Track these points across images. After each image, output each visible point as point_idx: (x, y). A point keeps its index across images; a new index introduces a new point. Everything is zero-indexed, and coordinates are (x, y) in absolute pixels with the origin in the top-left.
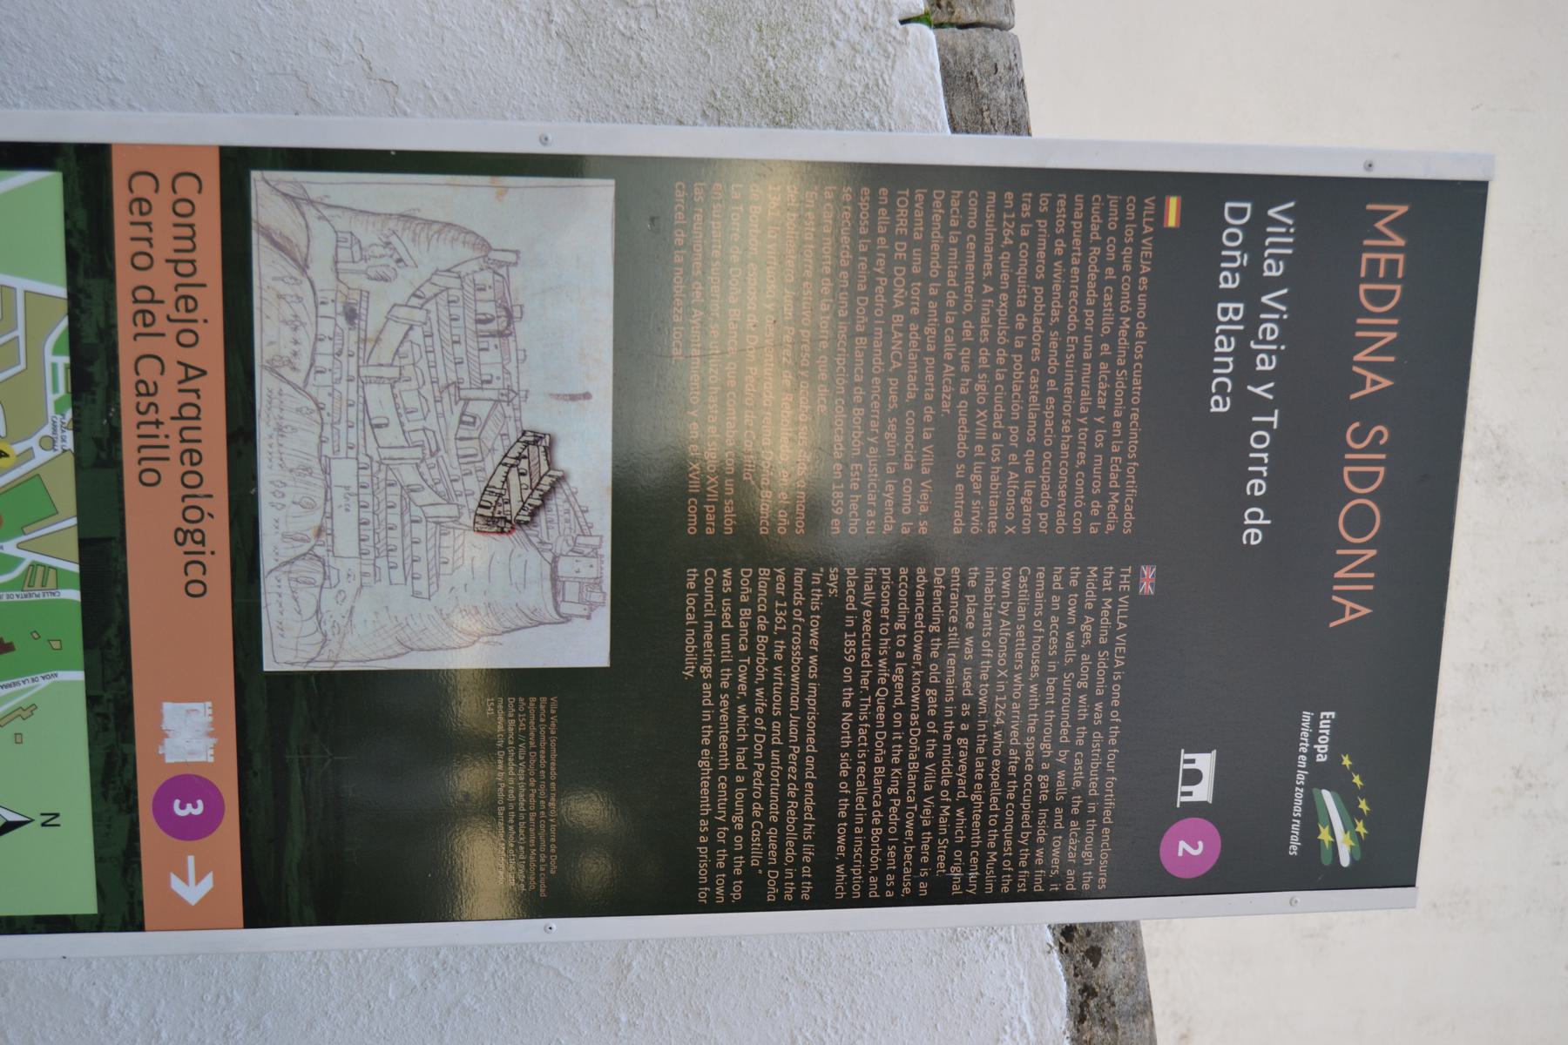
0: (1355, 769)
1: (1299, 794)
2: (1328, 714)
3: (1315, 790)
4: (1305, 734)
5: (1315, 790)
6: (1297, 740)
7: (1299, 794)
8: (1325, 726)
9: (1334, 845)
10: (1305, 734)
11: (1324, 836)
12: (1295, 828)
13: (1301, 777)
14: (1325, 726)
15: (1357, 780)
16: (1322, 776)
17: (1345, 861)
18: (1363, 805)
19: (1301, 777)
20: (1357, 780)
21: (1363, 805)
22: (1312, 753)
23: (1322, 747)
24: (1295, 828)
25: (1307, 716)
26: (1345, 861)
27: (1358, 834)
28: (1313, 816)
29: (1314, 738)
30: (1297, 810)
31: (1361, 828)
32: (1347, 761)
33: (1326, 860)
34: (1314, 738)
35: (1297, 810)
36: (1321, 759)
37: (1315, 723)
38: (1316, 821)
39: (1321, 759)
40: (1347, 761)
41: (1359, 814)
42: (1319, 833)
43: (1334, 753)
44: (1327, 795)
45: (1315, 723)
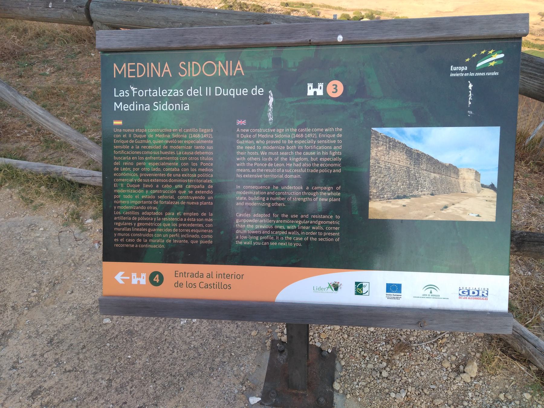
0: (470, 56)
1: (478, 74)
3: (477, 69)
4: (457, 75)
5: (477, 69)
6: (460, 77)
7: (478, 74)
8: (455, 69)
9: (496, 60)
10: (457, 75)
11: (492, 64)
12: (489, 74)
13: (472, 74)
14: (455, 69)
15: (474, 56)
16: (472, 67)
17: (502, 55)
18: (483, 52)
19: (472, 74)
20: (474, 56)
21: (483, 52)
22: (464, 72)
23: (462, 69)
24: (489, 74)
25: (452, 75)
26: (502, 55)
28: (485, 69)
30: (483, 74)
31: (491, 52)
32: (468, 60)
33: (501, 62)
34: (459, 72)
35: (483, 74)
36: (466, 68)
37: (454, 72)
39: (466, 68)
40: (468, 60)
43: (464, 65)
44: (478, 65)
45: (454, 72)
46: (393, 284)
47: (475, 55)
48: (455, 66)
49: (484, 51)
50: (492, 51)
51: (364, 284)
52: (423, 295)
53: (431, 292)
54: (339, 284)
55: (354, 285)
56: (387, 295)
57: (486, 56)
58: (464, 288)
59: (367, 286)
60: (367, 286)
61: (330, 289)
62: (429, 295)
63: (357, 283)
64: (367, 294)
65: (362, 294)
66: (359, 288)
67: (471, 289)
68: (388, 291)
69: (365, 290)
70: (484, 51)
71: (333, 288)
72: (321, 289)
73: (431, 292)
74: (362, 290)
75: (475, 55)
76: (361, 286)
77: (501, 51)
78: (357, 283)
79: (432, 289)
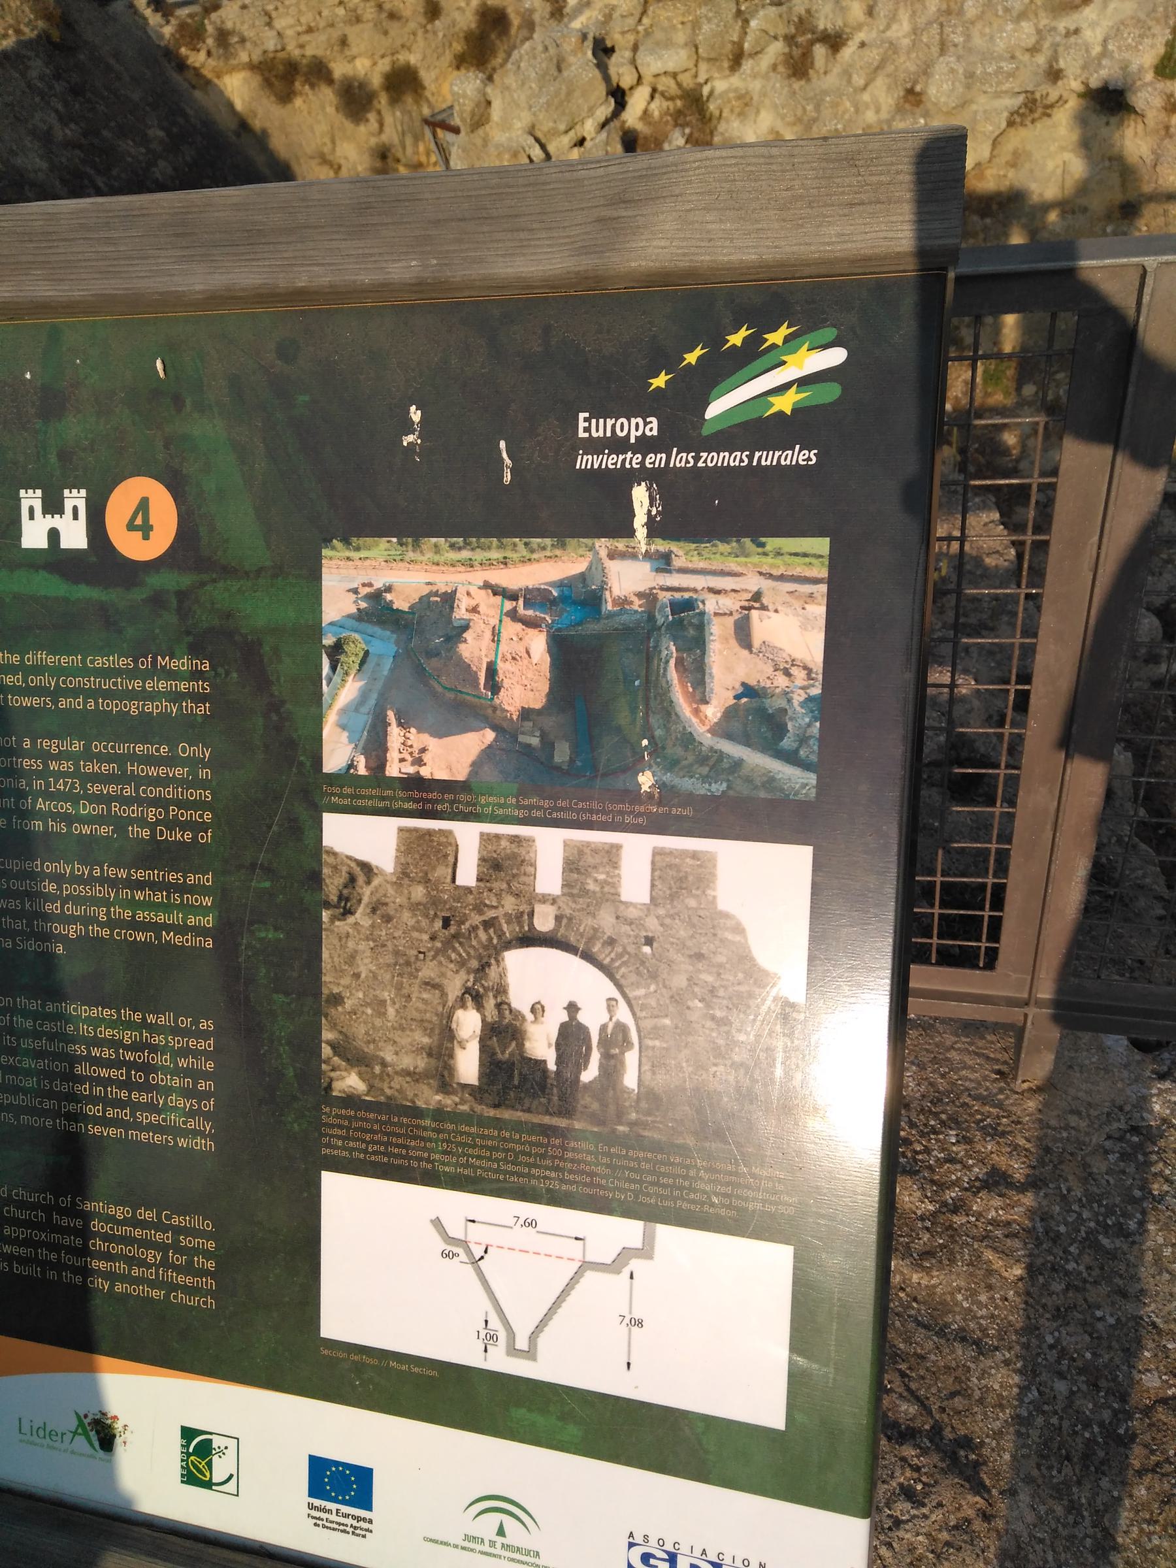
1: (711, 459)
2: (582, 424)
3: (706, 431)
5: (706, 431)
7: (711, 459)
8: (601, 429)
9: (803, 382)
11: (785, 404)
12: (767, 459)
13: (681, 460)
14: (601, 429)
15: (691, 358)
17: (836, 356)
18: (736, 340)
19: (681, 460)
20: (691, 358)
21: (736, 340)
22: (645, 445)
23: (636, 428)
24: (767, 459)
25: (585, 461)
26: (836, 356)
27: (787, 340)
28: (757, 429)
29: (618, 445)
30: (736, 459)
31: (776, 337)
32: (660, 381)
33: (831, 392)
34: (618, 445)
35: (736, 459)
36: (653, 427)
37: (595, 446)
38: (760, 420)
39: (653, 427)
40: (660, 381)
41: (753, 342)
42: (781, 414)
44: (714, 410)
45: (595, 446)
46: (337, 1464)
47: (698, 352)
48: (599, 412)
49: (743, 333)
50: (784, 331)
51: (217, 1442)
52: (467, 1538)
53: (501, 1532)
54: (119, 1426)
55: (177, 1440)
56: (311, 1507)
57: (752, 357)
58: (653, 1541)
59: (231, 1453)
60: (231, 1453)
61: (80, 1441)
62: (492, 1544)
63: (188, 1433)
64: (231, 1487)
65: (208, 1485)
66: (198, 1454)
67: (684, 1549)
68: (316, 1489)
69: (221, 1468)
70: (743, 333)
71: (93, 1434)
72: (46, 1433)
73: (501, 1532)
74: (209, 1465)
75: (698, 352)
76: (205, 1450)
77: (830, 333)
78: (188, 1433)
79: (510, 1524)
